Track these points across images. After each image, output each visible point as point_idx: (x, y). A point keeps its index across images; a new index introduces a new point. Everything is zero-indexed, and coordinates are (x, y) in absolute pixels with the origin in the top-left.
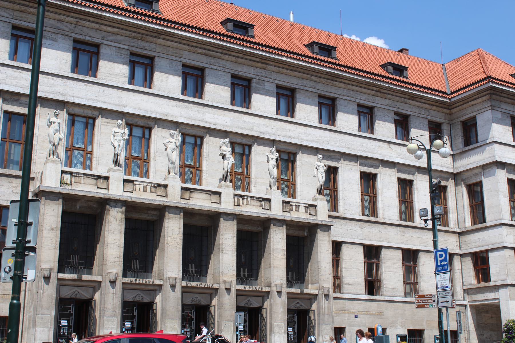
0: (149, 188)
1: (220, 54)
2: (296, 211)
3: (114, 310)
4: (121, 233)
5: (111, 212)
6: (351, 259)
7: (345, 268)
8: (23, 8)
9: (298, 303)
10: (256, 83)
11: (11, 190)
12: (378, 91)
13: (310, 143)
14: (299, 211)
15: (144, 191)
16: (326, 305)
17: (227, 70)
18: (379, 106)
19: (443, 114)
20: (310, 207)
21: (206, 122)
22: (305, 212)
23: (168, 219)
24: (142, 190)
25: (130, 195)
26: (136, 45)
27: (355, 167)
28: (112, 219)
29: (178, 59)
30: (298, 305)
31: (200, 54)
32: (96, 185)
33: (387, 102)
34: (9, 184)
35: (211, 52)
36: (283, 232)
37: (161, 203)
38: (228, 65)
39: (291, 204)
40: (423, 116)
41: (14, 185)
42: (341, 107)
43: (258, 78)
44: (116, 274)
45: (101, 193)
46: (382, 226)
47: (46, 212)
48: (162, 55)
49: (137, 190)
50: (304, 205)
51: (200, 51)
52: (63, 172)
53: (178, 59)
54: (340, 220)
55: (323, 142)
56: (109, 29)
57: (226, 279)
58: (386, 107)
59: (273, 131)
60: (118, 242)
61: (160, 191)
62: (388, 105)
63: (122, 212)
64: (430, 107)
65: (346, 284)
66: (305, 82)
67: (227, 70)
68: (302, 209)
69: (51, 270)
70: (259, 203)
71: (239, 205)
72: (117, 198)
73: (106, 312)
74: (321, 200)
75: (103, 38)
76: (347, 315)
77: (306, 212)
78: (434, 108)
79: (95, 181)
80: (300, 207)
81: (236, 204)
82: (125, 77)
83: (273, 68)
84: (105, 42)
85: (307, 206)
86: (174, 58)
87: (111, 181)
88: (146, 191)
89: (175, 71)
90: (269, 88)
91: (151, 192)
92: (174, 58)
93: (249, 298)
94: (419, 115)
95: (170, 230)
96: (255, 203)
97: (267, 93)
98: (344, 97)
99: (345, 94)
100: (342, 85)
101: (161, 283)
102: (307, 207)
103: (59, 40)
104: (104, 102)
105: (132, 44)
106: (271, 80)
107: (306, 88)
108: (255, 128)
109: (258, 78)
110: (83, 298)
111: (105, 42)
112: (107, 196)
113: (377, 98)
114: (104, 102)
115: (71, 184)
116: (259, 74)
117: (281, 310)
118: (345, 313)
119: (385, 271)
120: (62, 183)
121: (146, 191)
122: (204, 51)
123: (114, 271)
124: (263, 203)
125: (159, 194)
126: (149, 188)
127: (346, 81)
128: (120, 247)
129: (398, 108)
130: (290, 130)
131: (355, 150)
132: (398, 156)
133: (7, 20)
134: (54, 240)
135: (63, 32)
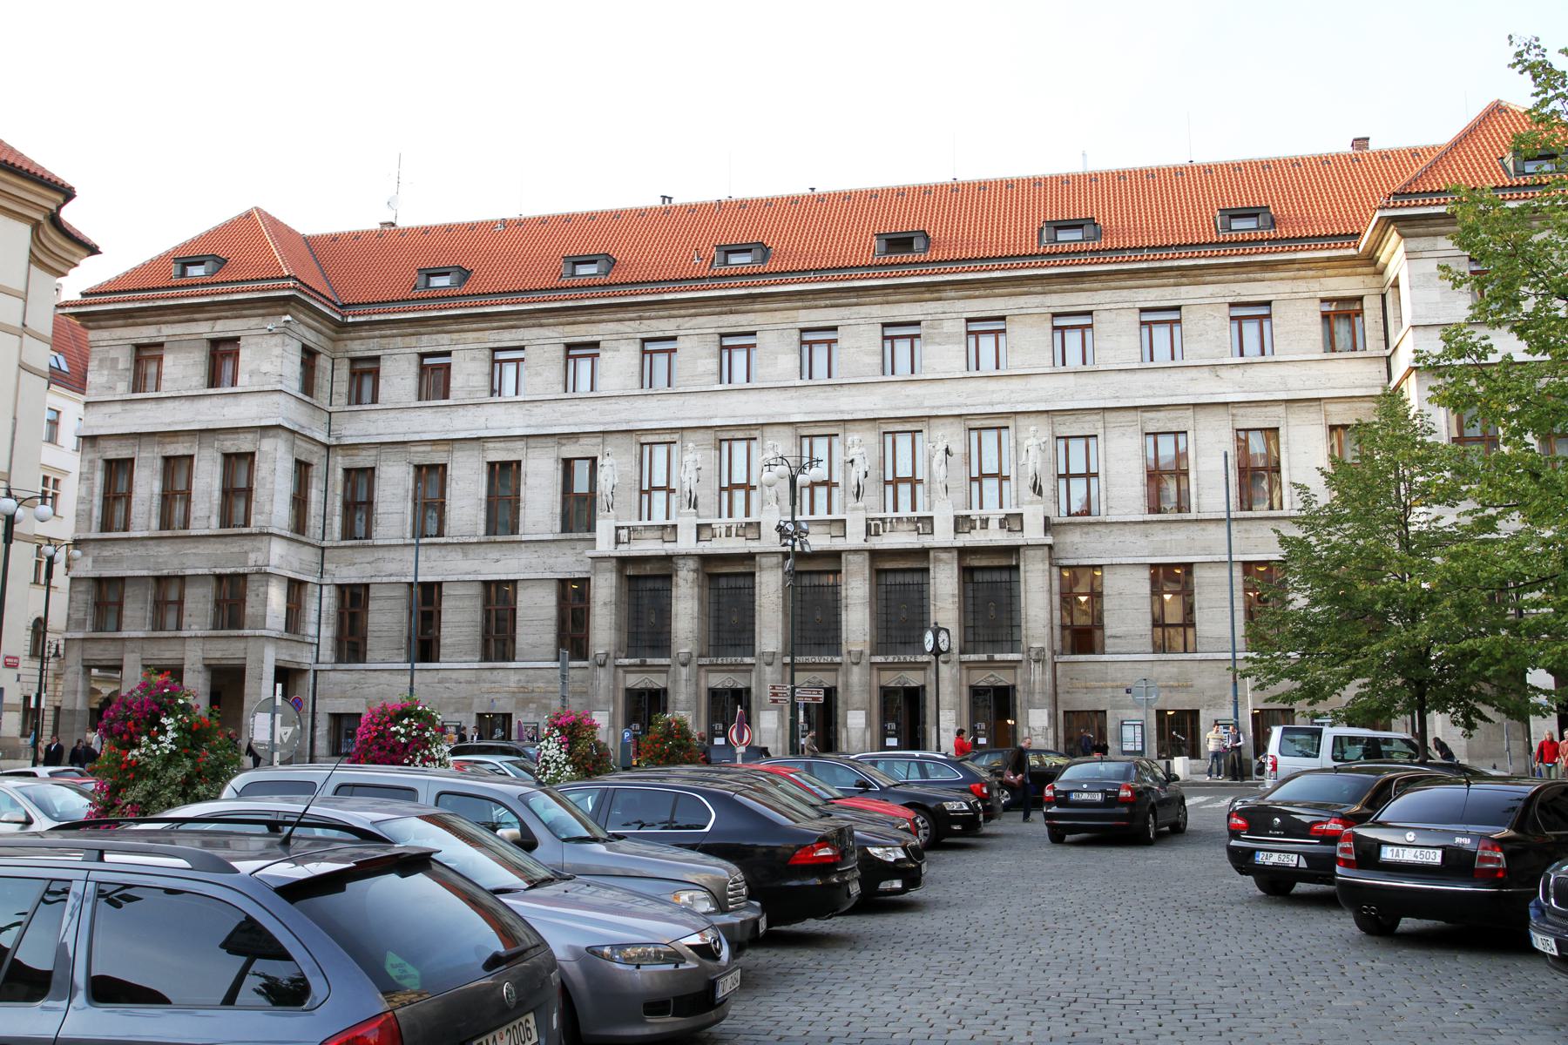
0: (734, 530)
1: (855, 300)
2: (982, 528)
3: (688, 702)
4: (693, 598)
5: (679, 573)
6: (1121, 594)
7: (1109, 610)
8: (571, 319)
9: (992, 676)
10: (927, 327)
11: (574, 559)
12: (1183, 276)
13: (1030, 405)
14: (987, 528)
15: (727, 536)
16: (1037, 678)
17: (874, 320)
18: (1191, 302)
19: (1360, 278)
20: (1011, 520)
21: (842, 412)
22: (1001, 528)
23: (760, 571)
24: (723, 535)
25: (707, 544)
26: (725, 324)
27: (1131, 429)
28: (681, 582)
29: (791, 325)
30: (992, 679)
31: (826, 307)
32: (662, 538)
33: (1210, 289)
34: (572, 551)
35: (840, 301)
36: (952, 569)
37: (746, 551)
38: (873, 312)
39: (973, 518)
40: (1306, 295)
41: (578, 551)
42: (1100, 325)
43: (930, 317)
44: (690, 653)
45: (669, 548)
46: (1195, 527)
47: (598, 583)
48: (765, 327)
49: (718, 535)
50: (998, 517)
51: (823, 303)
52: (617, 528)
53: (791, 325)
54: (1098, 528)
55: (1062, 397)
56: (683, 312)
57: (853, 648)
58: (1207, 301)
59: (961, 400)
60: (690, 612)
61: (751, 533)
62: (1212, 296)
63: (694, 571)
64: (1320, 273)
65: (1111, 637)
66: (1022, 300)
67: (874, 320)
68: (994, 524)
69: (607, 655)
70: (913, 527)
71: (877, 534)
72: (684, 552)
73: (678, 705)
74: (1031, 503)
75: (678, 328)
76: (1110, 690)
77: (1002, 527)
78: (1328, 272)
79: (659, 534)
80: (990, 522)
81: (873, 533)
82: (713, 374)
83: (953, 294)
84: (681, 332)
85: (1003, 516)
86: (784, 326)
87: (679, 530)
88: (730, 536)
89: (788, 345)
90: (952, 330)
91: (737, 535)
92: (784, 326)
93: (903, 674)
94: (1293, 296)
95: (763, 587)
96: (905, 526)
97: (949, 338)
98: (1108, 307)
99: (1108, 300)
100: (1098, 285)
101: (754, 662)
102: (1005, 519)
103: (622, 348)
104: (683, 419)
105: (720, 324)
106: (955, 315)
107: (1024, 311)
108: (926, 403)
109: (930, 317)
110: (656, 687)
111: (681, 332)
112: (670, 553)
113: (1183, 289)
114: (683, 419)
115: (629, 542)
116: (930, 312)
117: (950, 689)
118: (1107, 687)
119: (1200, 608)
120: (618, 542)
121: (730, 536)
122: (828, 302)
123: (686, 650)
124: (920, 525)
125: (749, 536)
126: (734, 530)
127: (1104, 277)
128: (693, 618)
129: (1239, 295)
130: (993, 392)
131: (1127, 398)
132: (1238, 389)
133: (557, 341)
134: (608, 618)
135: (625, 336)
